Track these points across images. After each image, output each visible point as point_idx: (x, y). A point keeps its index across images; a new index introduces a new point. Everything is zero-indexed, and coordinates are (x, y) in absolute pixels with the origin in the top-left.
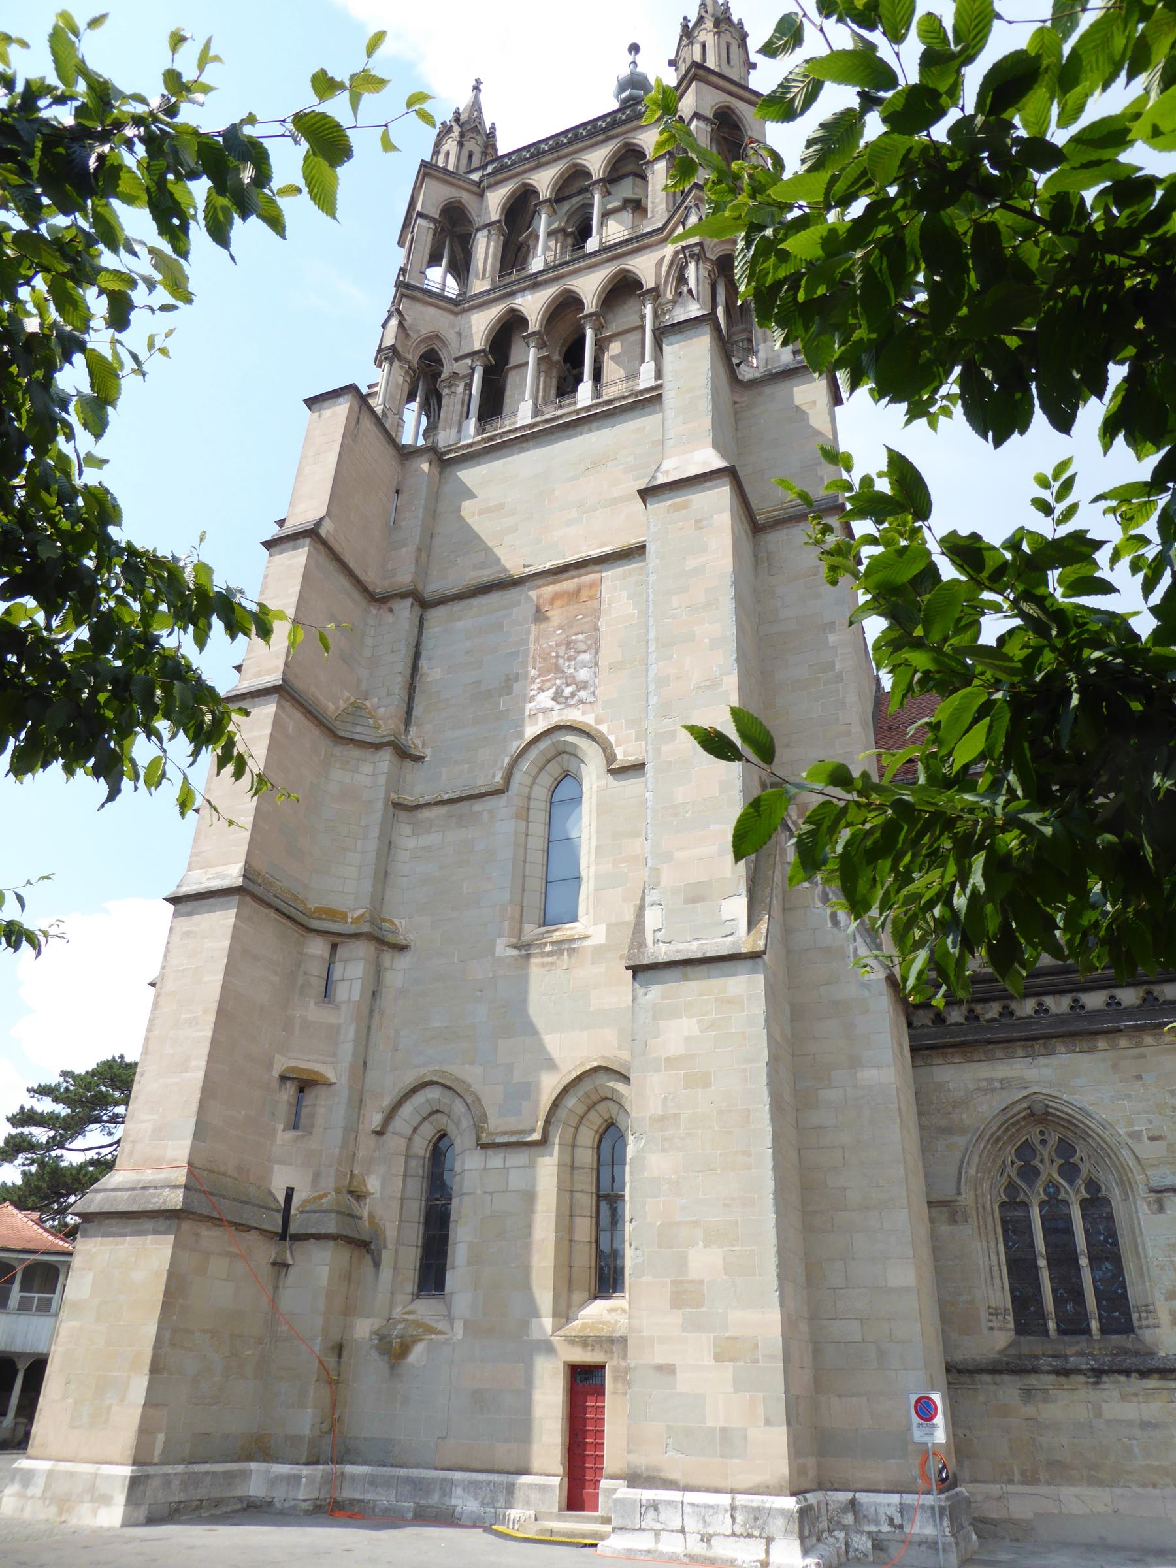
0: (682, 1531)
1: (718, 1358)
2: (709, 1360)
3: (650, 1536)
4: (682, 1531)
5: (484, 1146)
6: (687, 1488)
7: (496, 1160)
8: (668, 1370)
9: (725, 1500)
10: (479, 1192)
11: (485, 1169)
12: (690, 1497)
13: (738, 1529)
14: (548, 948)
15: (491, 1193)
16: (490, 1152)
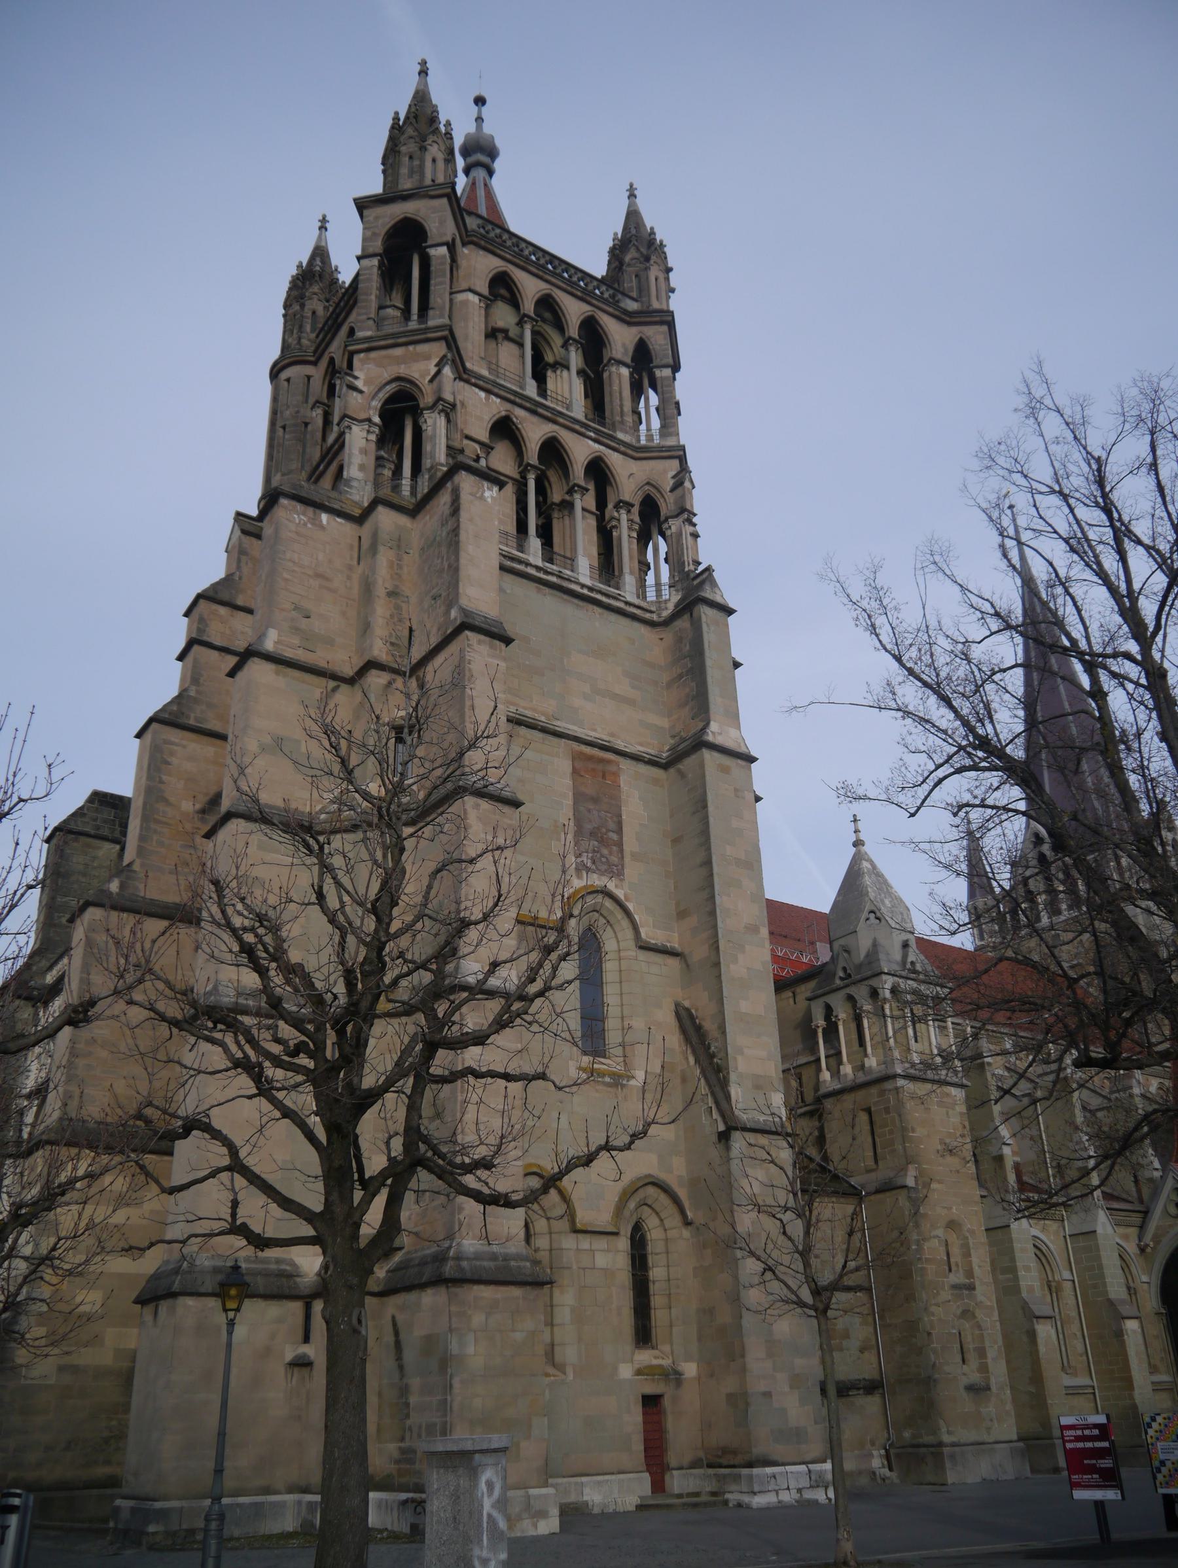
0: (788, 1489)
1: (791, 1387)
2: (787, 1389)
3: (774, 1494)
4: (788, 1489)
5: (576, 1231)
6: (783, 1464)
7: (585, 1242)
8: (768, 1395)
9: (803, 1468)
10: (575, 1267)
11: (577, 1249)
12: (789, 1468)
13: (813, 1483)
14: (607, 1079)
15: (584, 1269)
16: (580, 1236)
